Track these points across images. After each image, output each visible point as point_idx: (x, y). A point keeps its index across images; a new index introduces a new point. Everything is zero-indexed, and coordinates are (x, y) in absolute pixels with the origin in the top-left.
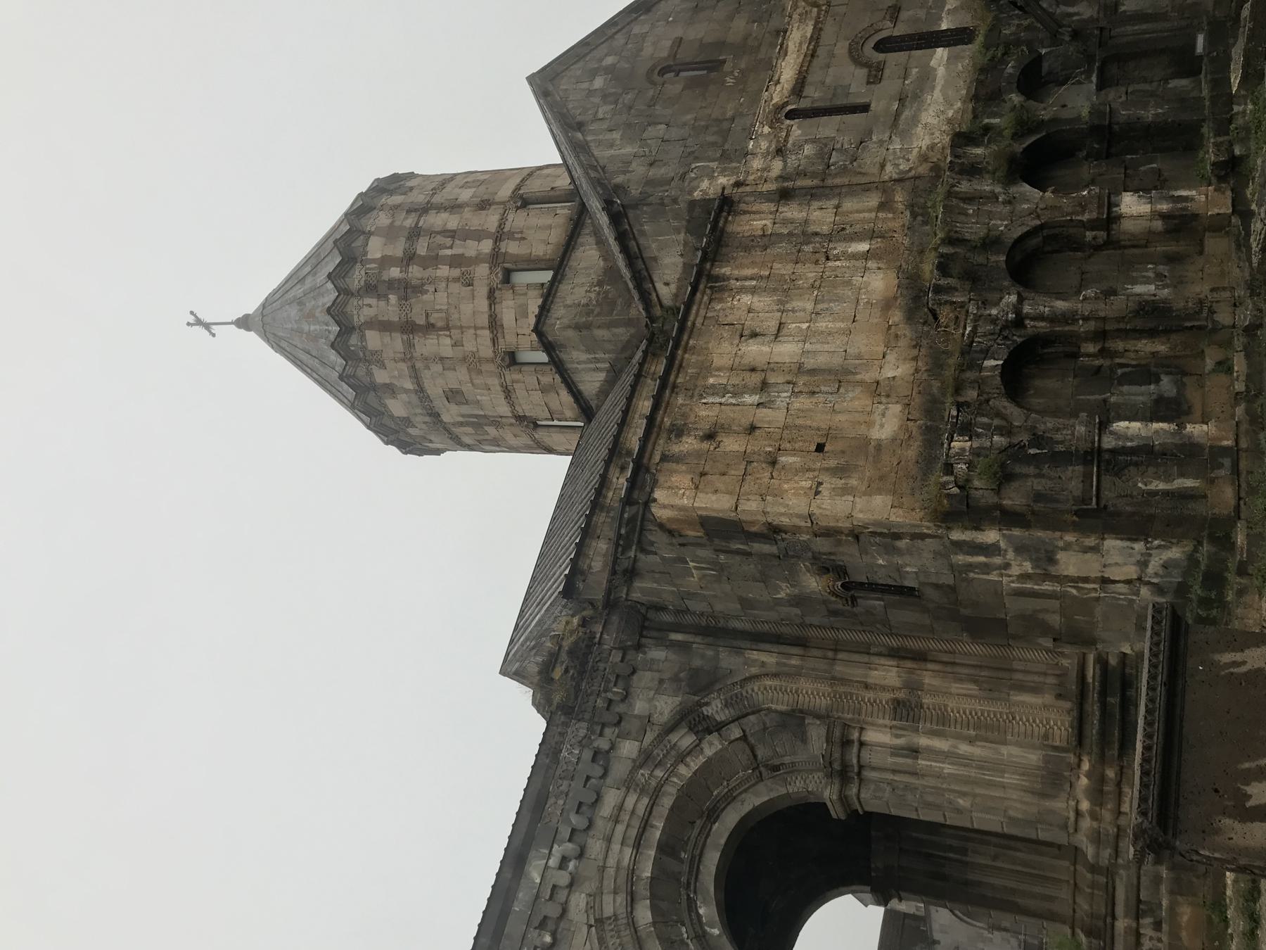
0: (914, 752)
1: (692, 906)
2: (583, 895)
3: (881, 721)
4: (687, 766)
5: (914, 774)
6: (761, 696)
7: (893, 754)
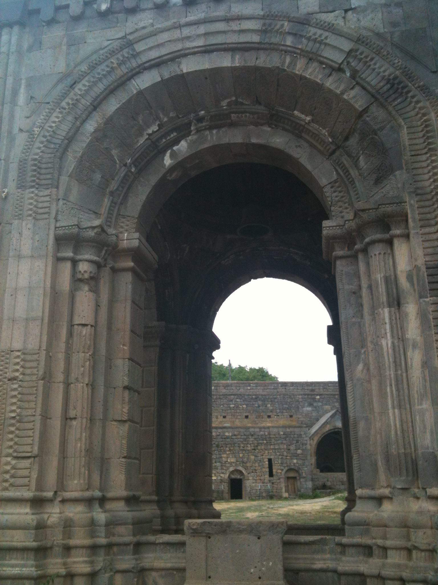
0: (396, 302)
1: (183, 130)
2: (151, 21)
3: (420, 252)
4: (306, 69)
5: (373, 308)
6: (413, 113)
7: (387, 280)
